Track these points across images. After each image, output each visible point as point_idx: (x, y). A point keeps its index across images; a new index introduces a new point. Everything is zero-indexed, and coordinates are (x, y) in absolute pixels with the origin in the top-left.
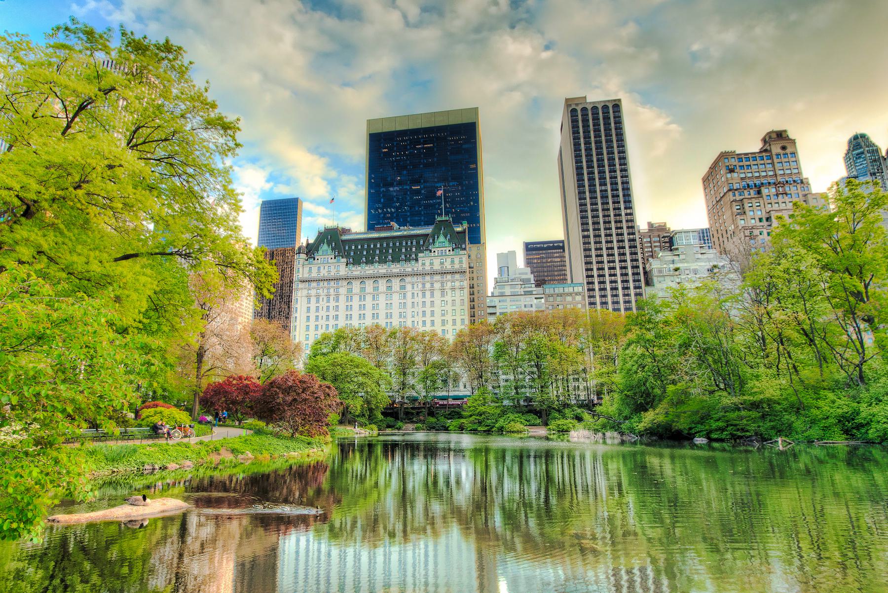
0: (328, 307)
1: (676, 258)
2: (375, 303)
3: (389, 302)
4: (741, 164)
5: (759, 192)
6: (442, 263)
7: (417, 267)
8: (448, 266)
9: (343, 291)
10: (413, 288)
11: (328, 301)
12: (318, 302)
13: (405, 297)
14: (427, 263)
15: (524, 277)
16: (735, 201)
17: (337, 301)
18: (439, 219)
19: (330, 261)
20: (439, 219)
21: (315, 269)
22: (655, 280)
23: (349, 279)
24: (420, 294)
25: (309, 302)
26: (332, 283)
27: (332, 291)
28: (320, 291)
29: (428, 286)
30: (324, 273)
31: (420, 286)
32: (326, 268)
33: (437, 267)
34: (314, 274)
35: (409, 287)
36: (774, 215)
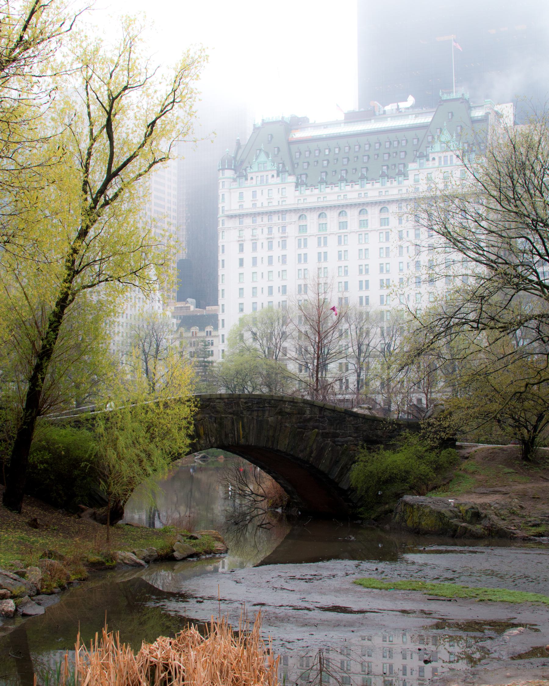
0: (270, 258)
2: (343, 248)
3: (363, 247)
9: (292, 231)
11: (270, 248)
12: (254, 249)
13: (387, 239)
17: (284, 246)
19: (271, 181)
23: (301, 213)
25: (241, 249)
26: (275, 218)
28: (258, 232)
30: (263, 202)
32: (266, 192)
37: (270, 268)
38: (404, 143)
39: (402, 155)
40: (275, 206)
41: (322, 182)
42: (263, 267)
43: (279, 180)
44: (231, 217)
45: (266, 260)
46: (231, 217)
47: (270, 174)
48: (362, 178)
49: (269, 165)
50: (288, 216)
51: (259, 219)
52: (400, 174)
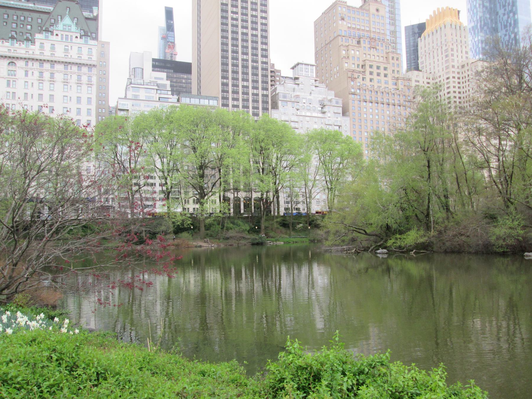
1: (296, 86)
4: (349, 15)
5: (359, 42)
6: (66, 50)
7: (34, 50)
8: (73, 56)
10: (26, 75)
14: (47, 46)
15: (159, 82)
16: (342, 45)
22: (280, 104)
24: (36, 84)
29: (47, 75)
31: (36, 74)
33: (59, 54)
35: (20, 73)
36: (368, 64)
52: (28, 40)
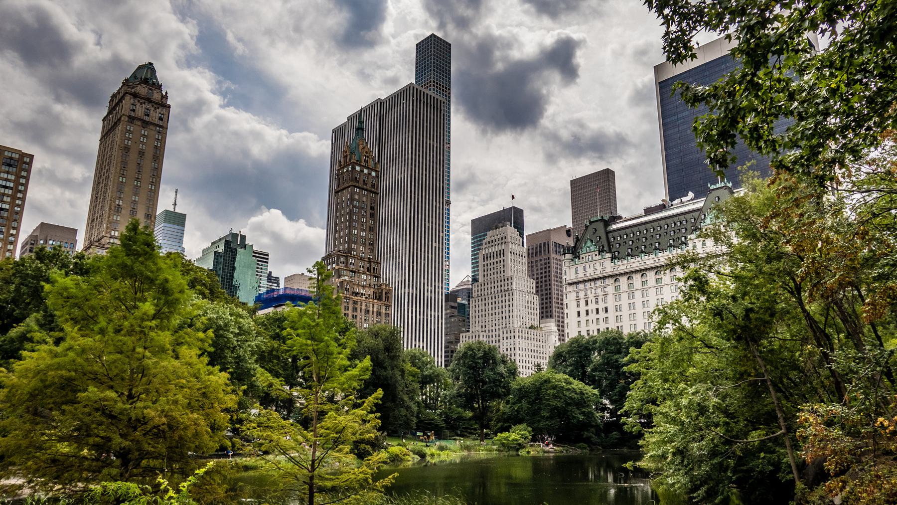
0: (597, 310)
2: (645, 299)
9: (610, 290)
12: (587, 304)
18: (712, 187)
19: (594, 258)
20: (712, 187)
21: (580, 269)
23: (615, 277)
25: (578, 306)
26: (599, 283)
27: (599, 291)
30: (590, 273)
32: (592, 266)
34: (581, 276)
37: (598, 316)
38: (684, 222)
39: (684, 230)
40: (598, 274)
41: (628, 255)
42: (593, 316)
43: (600, 257)
44: (570, 284)
45: (595, 311)
46: (570, 284)
47: (594, 254)
48: (656, 249)
49: (593, 248)
50: (607, 280)
51: (588, 284)
52: (682, 243)
